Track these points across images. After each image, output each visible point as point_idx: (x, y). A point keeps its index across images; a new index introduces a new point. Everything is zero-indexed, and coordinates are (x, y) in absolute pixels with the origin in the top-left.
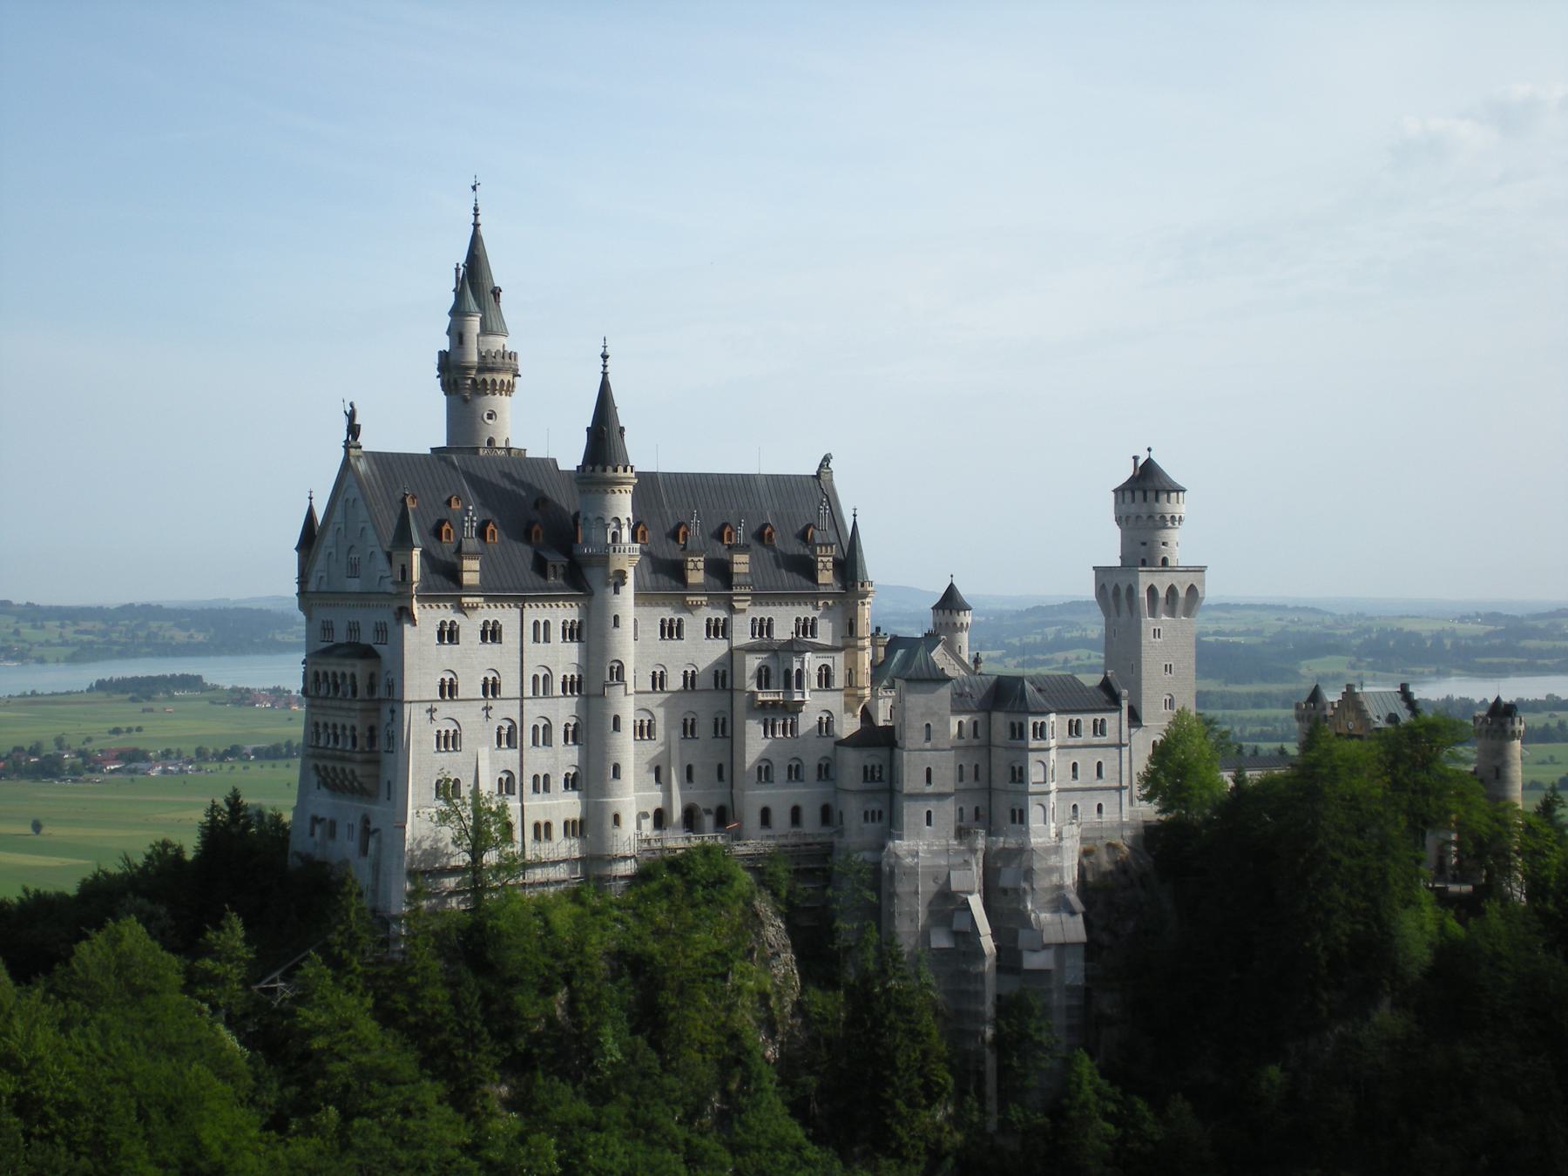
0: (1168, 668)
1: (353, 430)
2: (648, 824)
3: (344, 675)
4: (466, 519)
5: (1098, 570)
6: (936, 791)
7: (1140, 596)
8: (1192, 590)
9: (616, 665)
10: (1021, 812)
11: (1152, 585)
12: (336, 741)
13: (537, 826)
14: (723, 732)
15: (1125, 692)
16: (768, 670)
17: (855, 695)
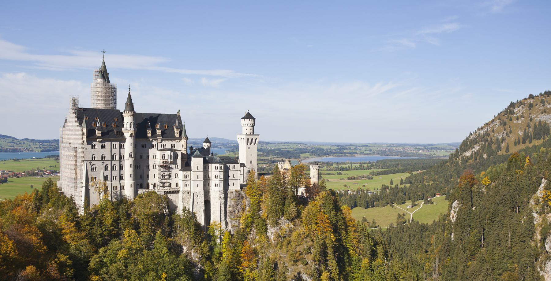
0: (251, 155)
1: (74, 104)
2: (139, 187)
4: (97, 122)
9: (131, 153)
13: (114, 187)
16: (164, 154)
17: (183, 160)
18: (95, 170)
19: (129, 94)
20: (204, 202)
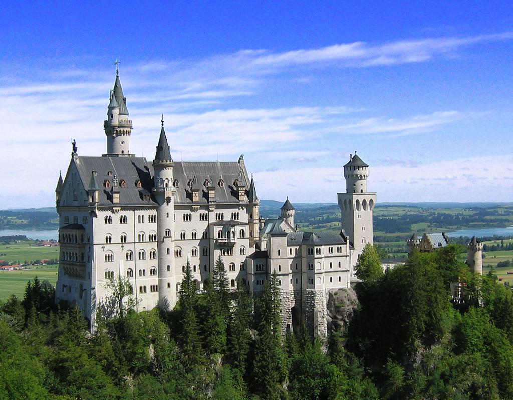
0: (363, 229)
1: (75, 149)
3: (72, 235)
6: (284, 273)
7: (353, 203)
8: (371, 201)
9: (168, 230)
10: (312, 280)
12: (70, 258)
13: (141, 288)
14: (206, 254)
15: (348, 237)
18: (110, 261)
19: (163, 131)
20: (291, 311)
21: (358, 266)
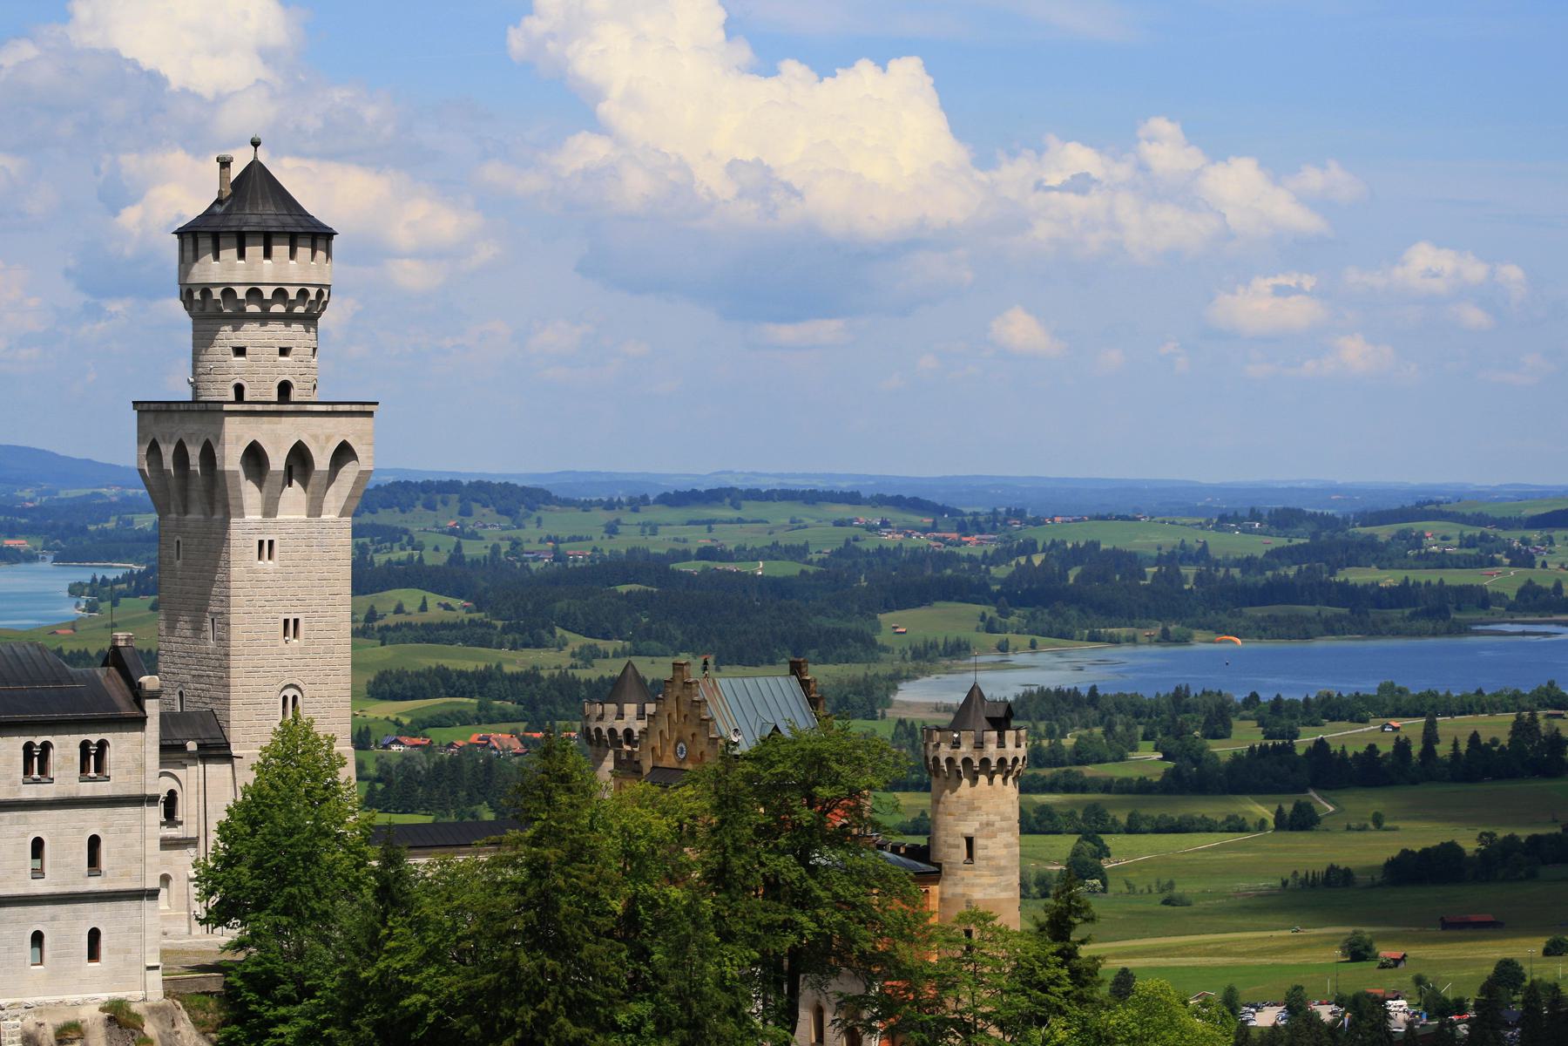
0: (291, 627)
5: (144, 409)
11: (300, 441)
15: (149, 681)
21: (229, 861)
